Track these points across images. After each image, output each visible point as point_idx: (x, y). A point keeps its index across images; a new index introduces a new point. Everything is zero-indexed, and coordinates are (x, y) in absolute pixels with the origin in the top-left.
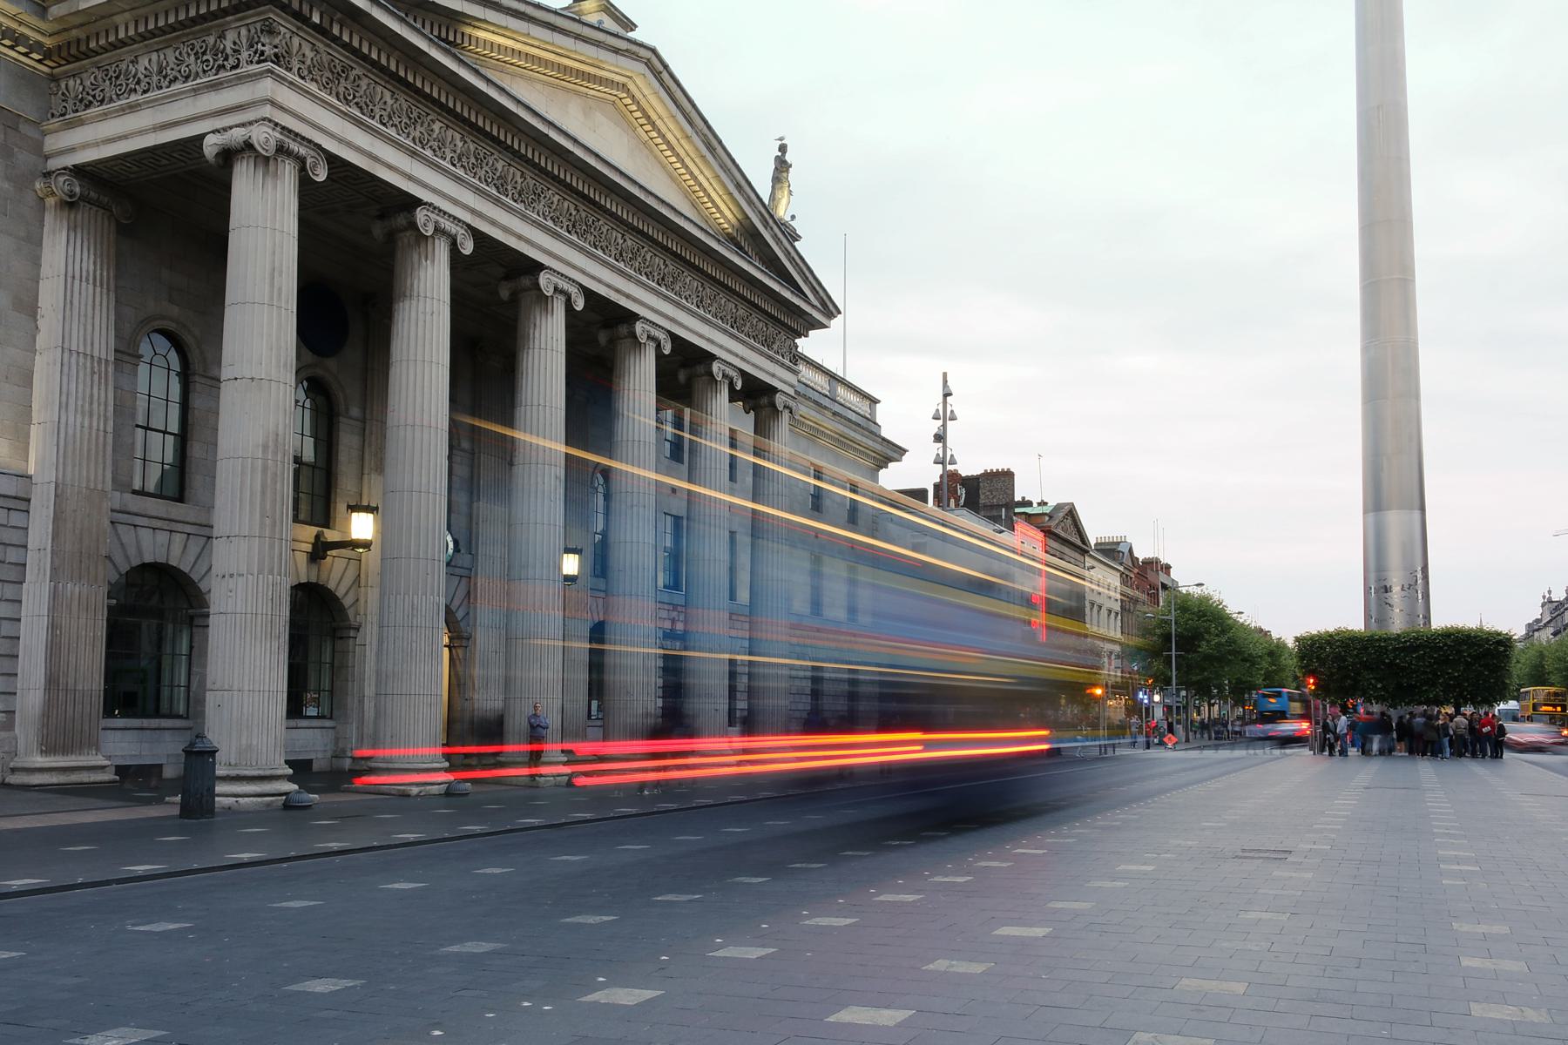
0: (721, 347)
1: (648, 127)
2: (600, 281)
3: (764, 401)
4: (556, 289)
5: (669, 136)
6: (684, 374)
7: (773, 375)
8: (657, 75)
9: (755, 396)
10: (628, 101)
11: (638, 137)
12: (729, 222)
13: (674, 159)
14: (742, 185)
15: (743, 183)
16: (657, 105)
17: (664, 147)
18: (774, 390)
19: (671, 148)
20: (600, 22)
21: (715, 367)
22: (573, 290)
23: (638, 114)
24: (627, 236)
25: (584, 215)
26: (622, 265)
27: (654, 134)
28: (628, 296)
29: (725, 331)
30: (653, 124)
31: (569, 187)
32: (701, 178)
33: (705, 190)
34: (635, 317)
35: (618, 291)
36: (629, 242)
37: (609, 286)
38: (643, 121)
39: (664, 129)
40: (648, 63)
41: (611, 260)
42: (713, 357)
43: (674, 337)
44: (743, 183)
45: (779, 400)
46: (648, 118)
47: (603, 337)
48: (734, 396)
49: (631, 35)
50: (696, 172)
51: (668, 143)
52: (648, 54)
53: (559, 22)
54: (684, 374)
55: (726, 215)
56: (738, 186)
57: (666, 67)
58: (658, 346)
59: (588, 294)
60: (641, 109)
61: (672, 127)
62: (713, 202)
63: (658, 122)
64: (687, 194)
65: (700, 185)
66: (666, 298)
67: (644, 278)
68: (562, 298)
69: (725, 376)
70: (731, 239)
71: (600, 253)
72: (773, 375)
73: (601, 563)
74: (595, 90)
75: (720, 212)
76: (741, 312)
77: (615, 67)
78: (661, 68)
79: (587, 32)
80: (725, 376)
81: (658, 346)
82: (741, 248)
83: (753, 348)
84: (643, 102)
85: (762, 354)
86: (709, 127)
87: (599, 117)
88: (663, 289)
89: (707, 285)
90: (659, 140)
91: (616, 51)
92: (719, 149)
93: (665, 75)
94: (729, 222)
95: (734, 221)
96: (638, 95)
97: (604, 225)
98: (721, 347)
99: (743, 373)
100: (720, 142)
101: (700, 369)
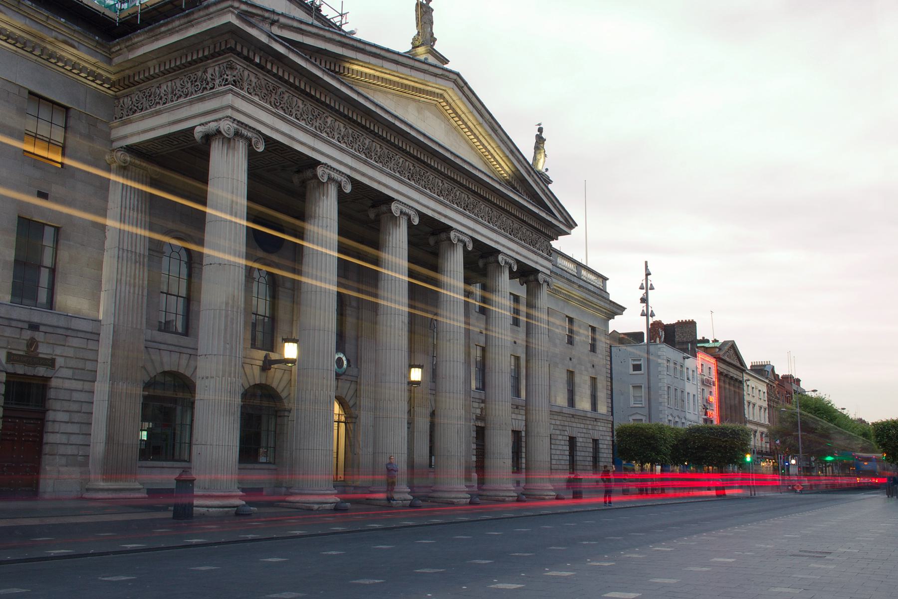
0: (504, 246)
1: (457, 119)
2: (428, 208)
3: (532, 278)
4: (401, 212)
5: (469, 124)
6: (481, 263)
7: (537, 263)
8: (461, 89)
9: (525, 274)
10: (444, 104)
11: (451, 124)
12: (507, 173)
13: (472, 137)
14: (513, 151)
15: (514, 150)
16: (461, 106)
17: (466, 130)
18: (538, 271)
19: (471, 131)
20: (426, 59)
21: (500, 257)
22: (412, 213)
23: (450, 111)
24: (445, 181)
25: (418, 169)
26: (442, 198)
27: (460, 123)
28: (446, 216)
29: (506, 237)
30: (459, 117)
31: (408, 153)
32: (489, 147)
33: (492, 155)
34: (450, 228)
35: (440, 213)
36: (446, 185)
37: (434, 210)
38: (453, 115)
39: (466, 119)
40: (455, 82)
41: (435, 195)
42: (499, 252)
43: (474, 240)
44: (514, 150)
45: (541, 277)
46: (456, 113)
47: (432, 241)
48: (512, 275)
49: (445, 66)
50: (486, 144)
51: (469, 128)
52: (455, 77)
53: (401, 59)
54: (481, 263)
55: (505, 168)
56: (512, 152)
57: (466, 84)
58: (465, 246)
59: (422, 215)
60: (451, 108)
61: (471, 119)
62: (497, 161)
63: (463, 116)
64: (481, 157)
65: (489, 151)
66: (469, 217)
67: (455, 206)
68: (406, 218)
69: (506, 263)
70: (508, 183)
71: (428, 191)
72: (537, 263)
73: (433, 375)
74: (424, 98)
76: (516, 225)
77: (435, 85)
78: (463, 84)
79: (417, 64)
80: (506, 263)
81: (465, 246)
82: (514, 188)
83: (523, 247)
84: (453, 104)
85: (529, 250)
86: (493, 118)
88: (467, 212)
90: (463, 126)
91: (436, 75)
93: (465, 89)
95: (510, 172)
96: (450, 101)
97: (431, 176)
98: (504, 246)
99: (518, 261)
100: (500, 126)
101: (492, 259)
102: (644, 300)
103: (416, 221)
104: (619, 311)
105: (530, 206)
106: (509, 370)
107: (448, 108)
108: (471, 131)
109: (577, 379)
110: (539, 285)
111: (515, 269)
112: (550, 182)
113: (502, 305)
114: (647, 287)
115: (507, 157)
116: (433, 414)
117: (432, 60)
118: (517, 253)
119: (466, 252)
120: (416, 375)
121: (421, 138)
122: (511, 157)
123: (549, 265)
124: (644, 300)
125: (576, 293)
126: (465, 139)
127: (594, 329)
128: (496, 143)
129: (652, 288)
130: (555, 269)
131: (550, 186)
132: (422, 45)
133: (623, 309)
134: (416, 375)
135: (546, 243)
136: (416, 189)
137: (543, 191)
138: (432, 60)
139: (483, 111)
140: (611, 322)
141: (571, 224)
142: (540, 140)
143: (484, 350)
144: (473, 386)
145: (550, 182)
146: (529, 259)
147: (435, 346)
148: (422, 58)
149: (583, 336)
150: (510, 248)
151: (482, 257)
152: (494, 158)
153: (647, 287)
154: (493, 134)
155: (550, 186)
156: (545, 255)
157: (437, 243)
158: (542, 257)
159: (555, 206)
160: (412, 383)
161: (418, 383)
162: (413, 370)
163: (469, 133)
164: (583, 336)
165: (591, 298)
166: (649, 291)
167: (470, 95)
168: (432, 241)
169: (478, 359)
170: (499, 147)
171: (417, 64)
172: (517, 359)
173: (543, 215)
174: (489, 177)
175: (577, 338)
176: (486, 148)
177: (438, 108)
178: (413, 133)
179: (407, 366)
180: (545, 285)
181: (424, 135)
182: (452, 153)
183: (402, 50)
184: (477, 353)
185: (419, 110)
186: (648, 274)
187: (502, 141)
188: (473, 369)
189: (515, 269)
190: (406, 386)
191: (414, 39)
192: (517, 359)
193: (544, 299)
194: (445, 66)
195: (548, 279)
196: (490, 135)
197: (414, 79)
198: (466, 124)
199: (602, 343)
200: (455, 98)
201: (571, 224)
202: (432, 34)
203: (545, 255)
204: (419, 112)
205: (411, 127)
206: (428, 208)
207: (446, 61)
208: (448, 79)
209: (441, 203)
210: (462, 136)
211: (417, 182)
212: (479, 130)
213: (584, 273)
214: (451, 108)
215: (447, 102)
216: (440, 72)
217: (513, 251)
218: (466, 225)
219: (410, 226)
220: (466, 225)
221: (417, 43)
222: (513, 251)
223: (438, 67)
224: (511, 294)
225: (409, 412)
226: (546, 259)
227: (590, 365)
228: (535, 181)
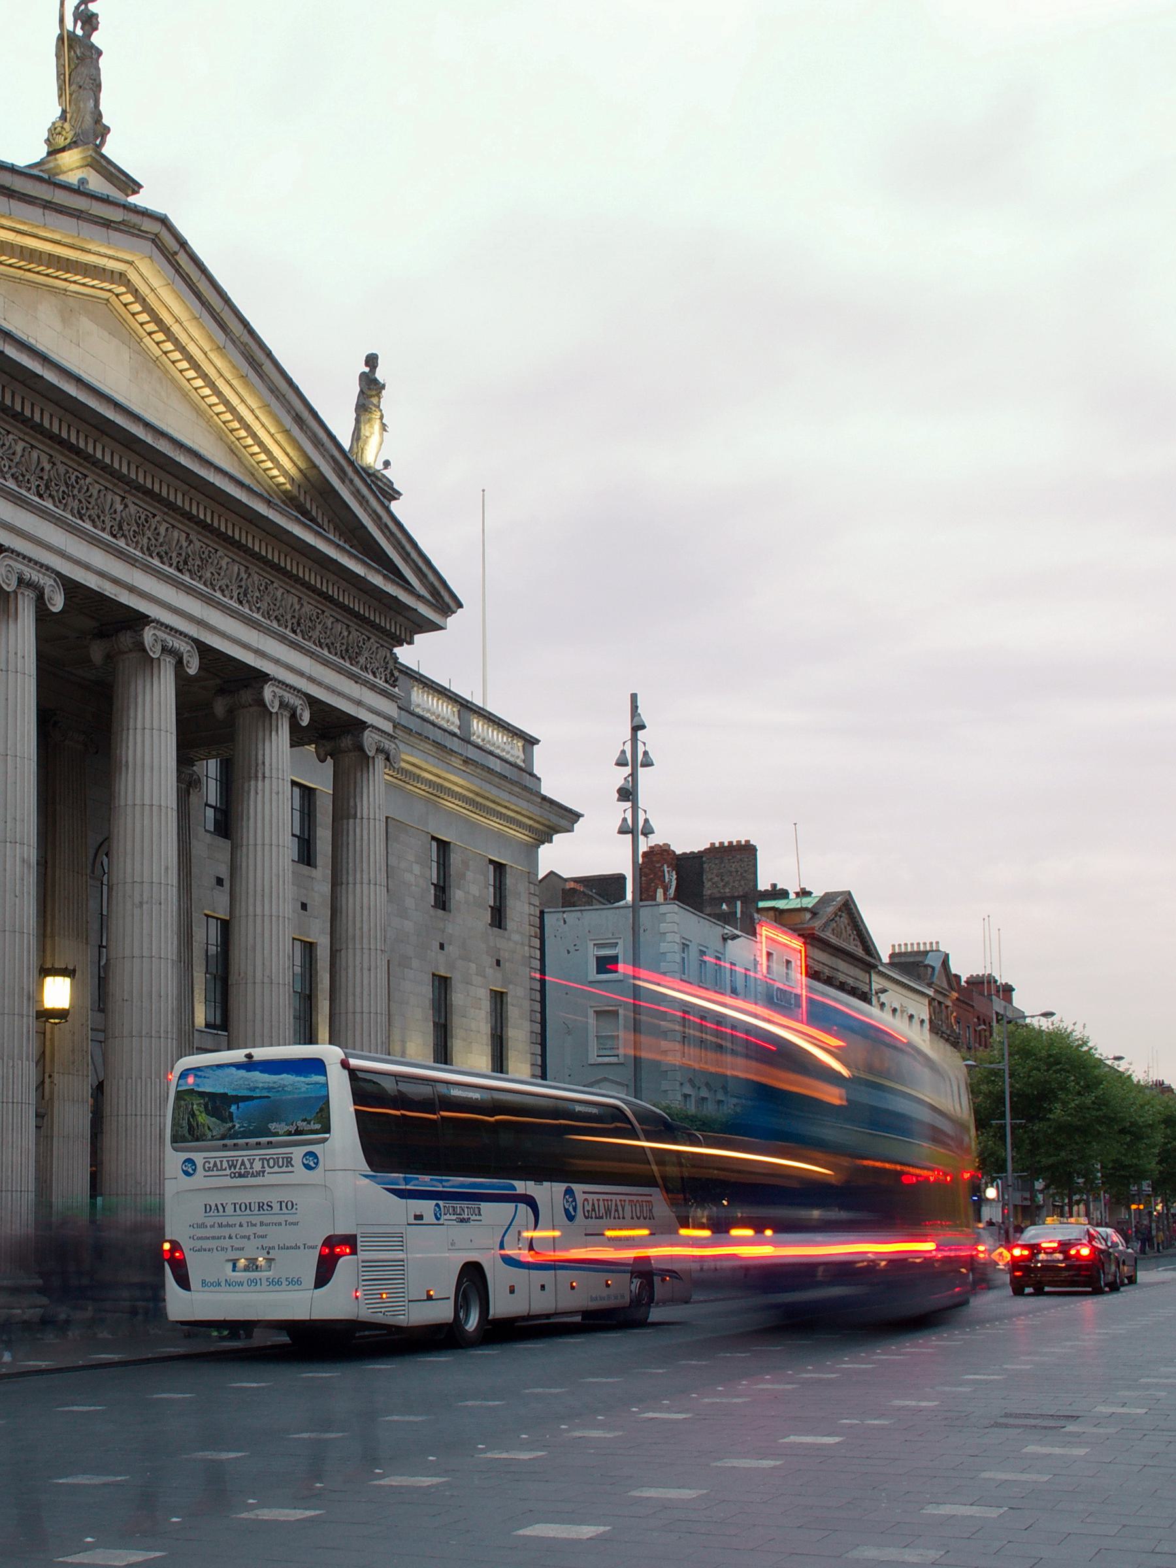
0: (277, 662)
1: (160, 337)
2: (87, 567)
3: (347, 742)
4: (20, 581)
5: (192, 349)
6: (220, 706)
7: (359, 703)
8: (170, 258)
9: (331, 732)
10: (129, 298)
11: (145, 352)
12: (285, 473)
13: (199, 383)
14: (301, 417)
15: (306, 415)
16: (172, 304)
17: (184, 365)
18: (362, 725)
19: (196, 366)
20: (83, 181)
21: (268, 692)
22: (47, 582)
23: (144, 317)
24: (130, 499)
25: (62, 469)
26: (122, 543)
27: (169, 346)
28: (132, 589)
29: (283, 639)
30: (166, 330)
31: (38, 429)
32: (242, 410)
33: (247, 427)
34: (143, 620)
35: (116, 581)
36: (132, 509)
37: (102, 574)
38: (151, 327)
39: (183, 338)
40: (156, 241)
41: (106, 536)
42: (264, 677)
43: (203, 649)
44: (306, 415)
45: (369, 740)
46: (158, 321)
47: (97, 651)
48: (299, 737)
49: (133, 199)
50: (234, 401)
51: (189, 358)
52: (155, 227)
53: (19, 184)
54: (220, 706)
55: (279, 459)
56: (299, 420)
57: (183, 244)
58: (179, 664)
59: (71, 588)
60: (147, 308)
61: (195, 335)
62: (260, 444)
63: (176, 329)
64: (220, 435)
65: (241, 419)
66: (190, 591)
67: (156, 562)
68: (31, 594)
69: (283, 705)
70: (291, 502)
71: (88, 526)
72: (359, 703)
73: (100, 992)
74: (77, 284)
75: (272, 458)
76: (307, 609)
77: (102, 251)
78: (173, 245)
79: (61, 197)
80: (283, 705)
81: (179, 664)
82: (305, 513)
83: (326, 663)
84: (151, 299)
85: (340, 670)
86: (251, 332)
87: (85, 323)
88: (186, 578)
89: (253, 569)
90: (177, 355)
91: (107, 224)
92: (268, 367)
93: (182, 259)
94: (285, 473)
95: (293, 471)
96: (143, 289)
97: (93, 484)
98: (277, 662)
99: (312, 701)
100: (269, 354)
101: (246, 696)
102: (627, 794)
103: (57, 603)
104: (563, 823)
105: (343, 558)
106: (288, 978)
107: (137, 308)
108: (196, 366)
109: (458, 998)
110: (365, 761)
111: (305, 720)
112: (394, 495)
113: (272, 814)
114: (635, 760)
115: (287, 432)
116: (99, 1090)
117: (97, 184)
118: (311, 679)
119: (183, 682)
120: (57, 993)
121: (71, 389)
122: (296, 431)
123: (390, 708)
124: (627, 794)
125: (457, 781)
126: (180, 389)
127: (499, 868)
128: (260, 398)
129: (648, 763)
130: (406, 719)
131: (394, 506)
132: (73, 144)
133: (578, 816)
134: (57, 993)
135: (382, 652)
136: (58, 522)
137: (377, 519)
138: (97, 184)
139: (227, 315)
140: (544, 850)
141: (445, 601)
142: (370, 387)
143: (226, 926)
144: (200, 1019)
145: (394, 495)
146: (340, 694)
147: (104, 921)
148: (73, 178)
149: (473, 889)
150: (294, 667)
151: (222, 691)
152: (254, 436)
153: (635, 760)
154: (252, 374)
155: (394, 506)
156: (380, 682)
157: (110, 658)
158: (373, 687)
159: (406, 557)
160: (46, 1015)
161: (62, 1014)
162: (49, 981)
163: (191, 374)
164: (473, 889)
165: (494, 792)
166: (640, 770)
167: (195, 274)
168: (97, 651)
169: (213, 950)
170: (266, 406)
171: (61, 197)
172: (309, 948)
173: (377, 580)
174: (249, 489)
175: (457, 895)
176: (232, 409)
177: (113, 310)
178: (50, 376)
179: (35, 972)
180: (380, 761)
181: (78, 381)
182: (147, 425)
183: (22, 159)
184: (205, 936)
185: (66, 316)
186: (637, 727)
187: (274, 390)
188: (199, 977)
189: (305, 720)
190: (32, 1020)
191: (53, 131)
192: (309, 948)
193: (377, 794)
194: (133, 199)
195: (387, 744)
196: (243, 377)
197: (50, 237)
198: (182, 349)
199: (520, 910)
200: (156, 282)
201: (445, 601)
202: (98, 117)
203: (380, 682)
204: (65, 321)
205: (45, 359)
206: (87, 567)
207: (133, 186)
208: (140, 234)
209: (120, 554)
210: (173, 380)
211: (60, 501)
212: (218, 365)
213: (478, 727)
214: (147, 308)
215: (135, 292)
216: (116, 215)
217: (301, 674)
218: (181, 609)
219: (43, 615)
220: (181, 609)
221: (61, 142)
222: (301, 674)
223: (109, 204)
224: (294, 783)
225: (41, 1085)
226: (383, 693)
227: (489, 961)
228: (357, 494)
